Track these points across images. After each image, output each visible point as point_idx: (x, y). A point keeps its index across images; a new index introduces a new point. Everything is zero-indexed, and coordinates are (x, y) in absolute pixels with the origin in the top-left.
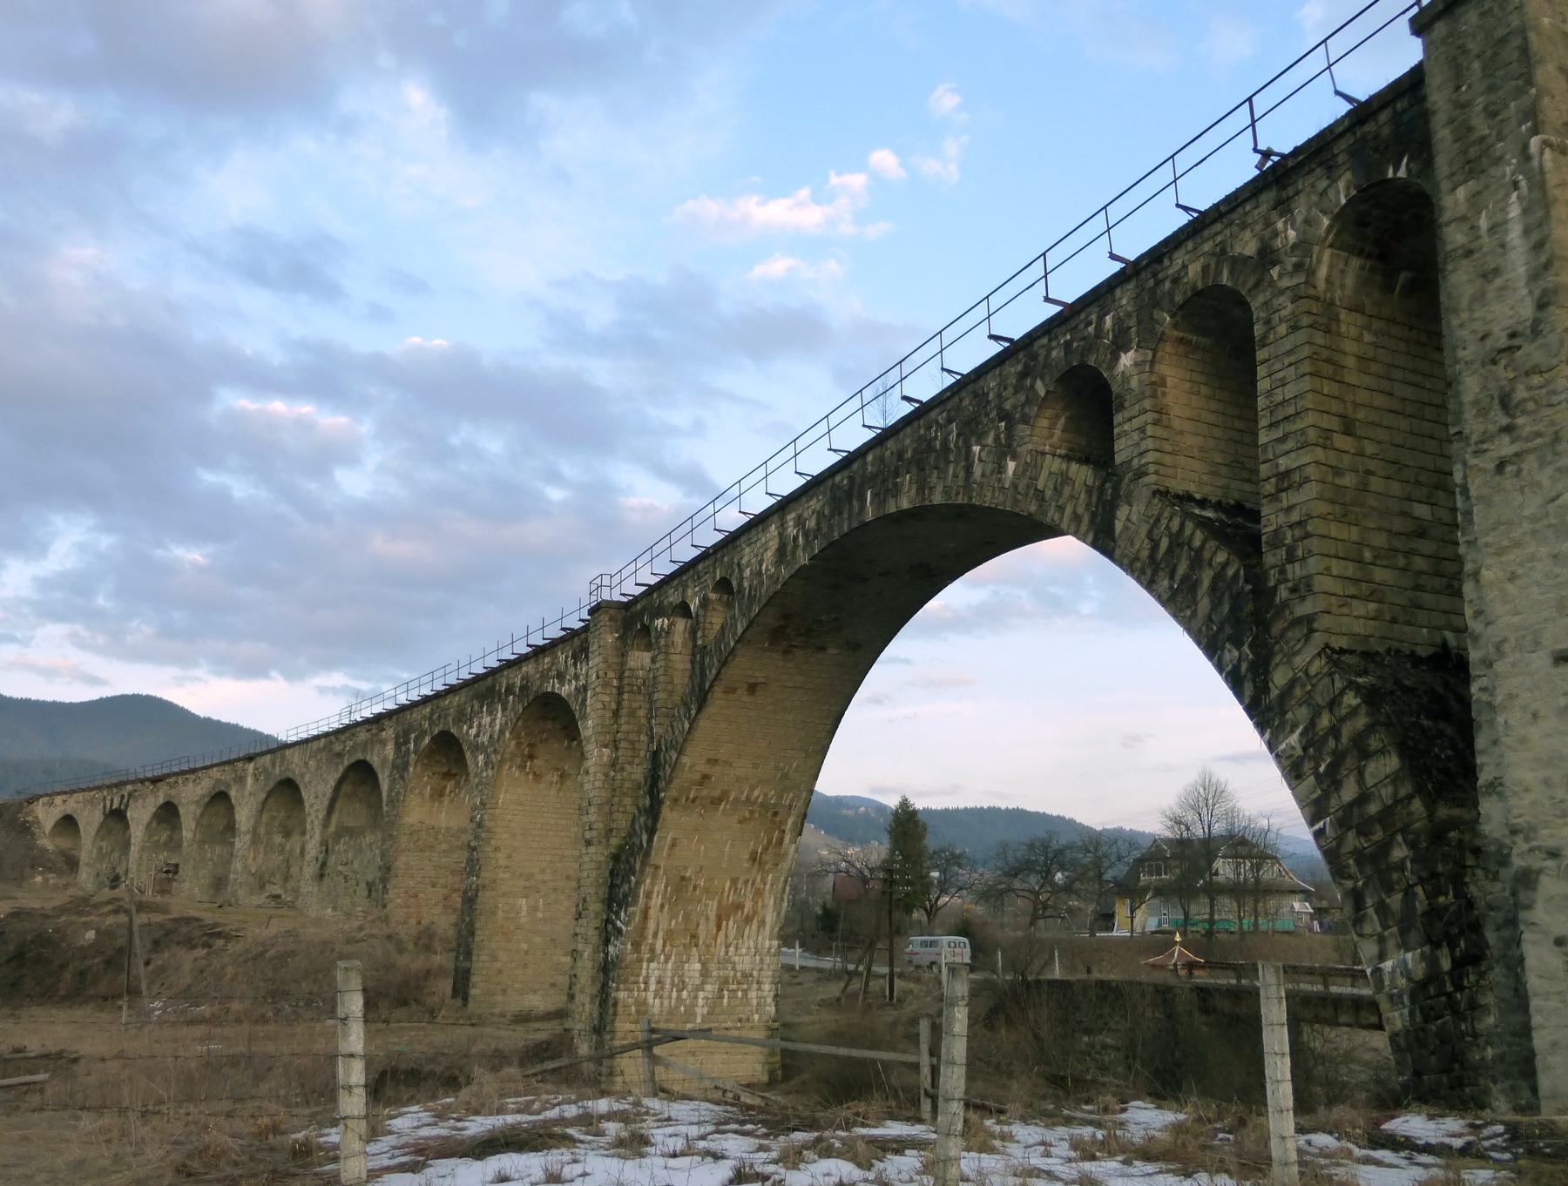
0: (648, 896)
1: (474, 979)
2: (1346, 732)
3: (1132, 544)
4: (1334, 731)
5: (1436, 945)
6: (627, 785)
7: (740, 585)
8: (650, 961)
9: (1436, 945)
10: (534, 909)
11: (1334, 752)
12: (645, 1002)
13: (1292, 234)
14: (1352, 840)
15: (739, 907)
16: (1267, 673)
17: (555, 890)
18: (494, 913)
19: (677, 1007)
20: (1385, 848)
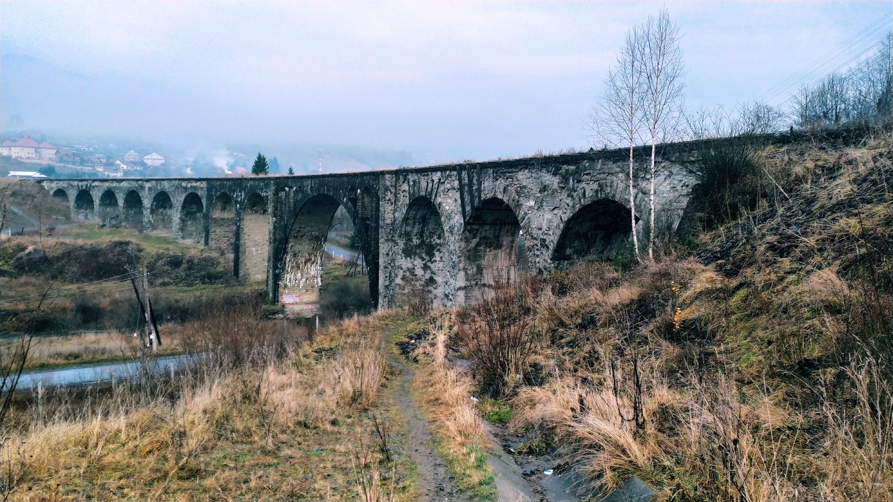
0: (286, 258)
15: (311, 259)
17: (263, 245)
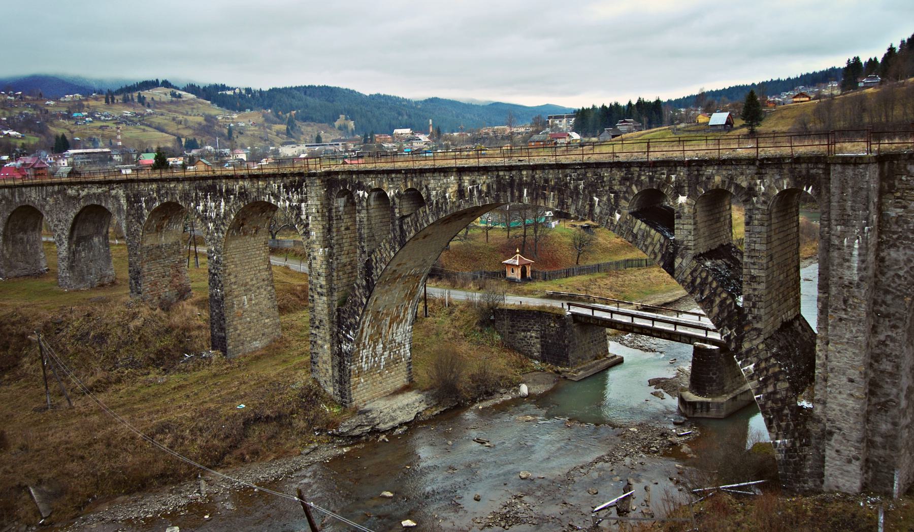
0: (364, 323)
1: (229, 341)
2: (771, 371)
3: (683, 274)
4: (767, 369)
5: (796, 439)
6: (340, 266)
7: (429, 196)
8: (363, 349)
9: (796, 439)
10: (251, 300)
11: (766, 375)
12: (361, 367)
13: (763, 188)
14: (770, 403)
16: (742, 342)
18: (233, 307)
19: (374, 365)
20: (782, 409)
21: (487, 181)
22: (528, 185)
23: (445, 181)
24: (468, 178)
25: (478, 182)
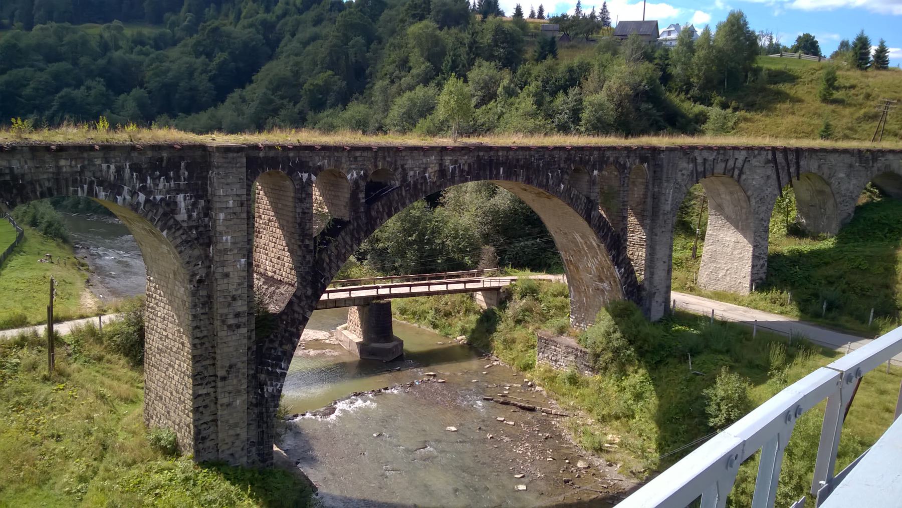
21: (469, 161)
22: (503, 164)
23: (424, 161)
24: (449, 158)
25: (460, 161)
